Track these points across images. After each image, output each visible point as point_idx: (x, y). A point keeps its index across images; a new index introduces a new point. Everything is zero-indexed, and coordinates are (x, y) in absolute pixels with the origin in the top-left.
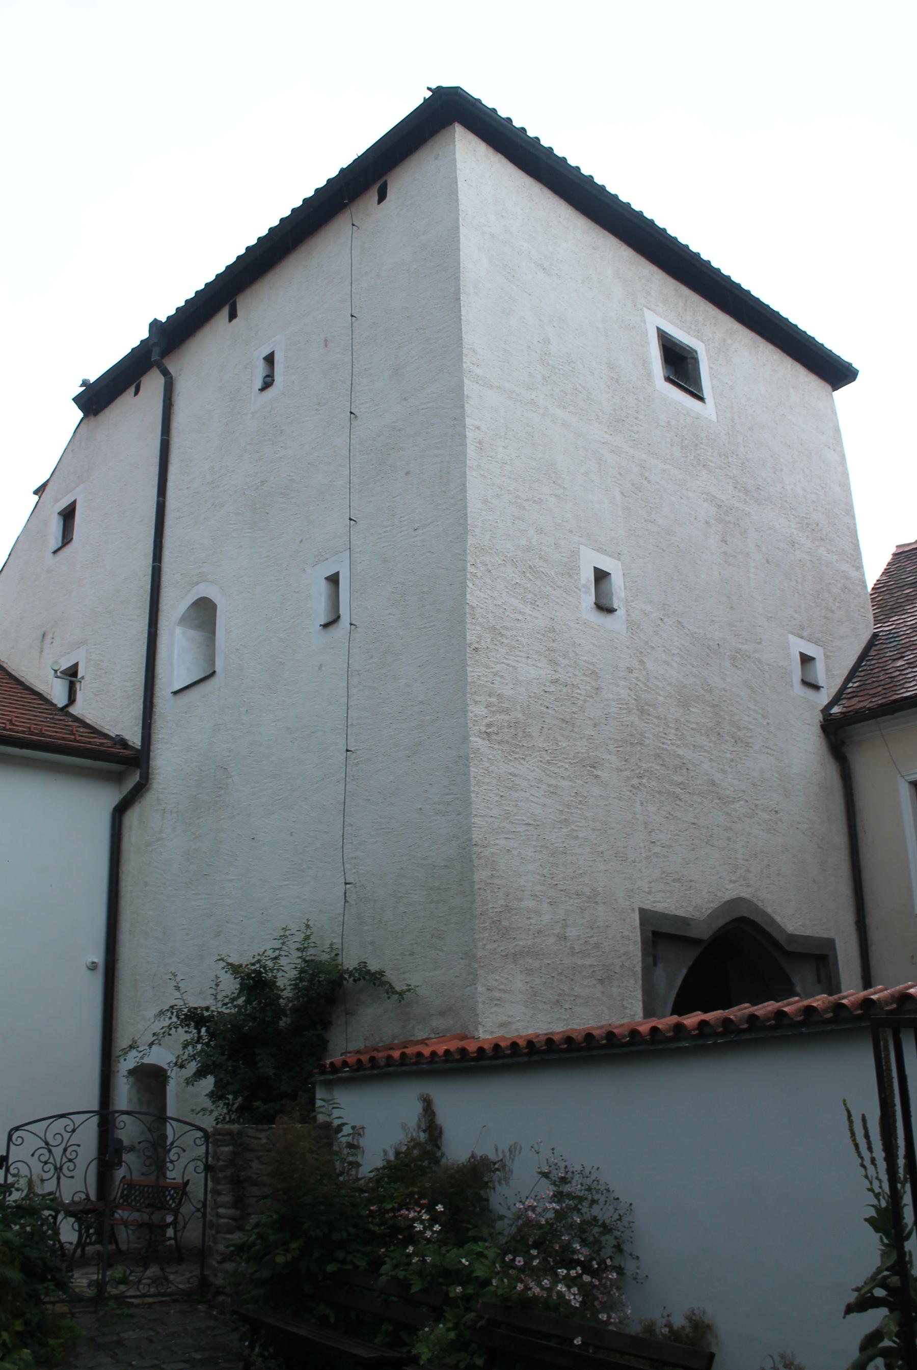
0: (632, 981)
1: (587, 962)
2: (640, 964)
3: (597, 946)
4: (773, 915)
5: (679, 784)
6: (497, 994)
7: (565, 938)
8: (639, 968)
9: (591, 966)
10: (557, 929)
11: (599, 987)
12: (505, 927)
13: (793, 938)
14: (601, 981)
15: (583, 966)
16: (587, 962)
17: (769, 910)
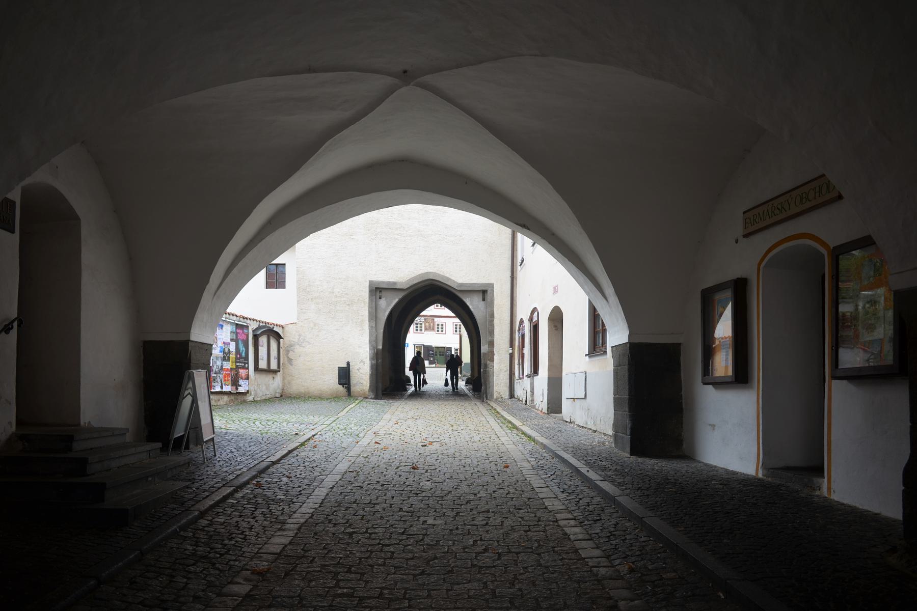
0: (363, 304)
1: (342, 299)
2: (368, 299)
3: (347, 294)
4: (450, 277)
5: (398, 235)
6: (304, 311)
7: (333, 292)
8: (367, 300)
9: (344, 301)
10: (330, 290)
11: (348, 307)
12: (308, 291)
13: (461, 285)
14: (348, 305)
15: (341, 301)
16: (342, 299)
17: (447, 275)
